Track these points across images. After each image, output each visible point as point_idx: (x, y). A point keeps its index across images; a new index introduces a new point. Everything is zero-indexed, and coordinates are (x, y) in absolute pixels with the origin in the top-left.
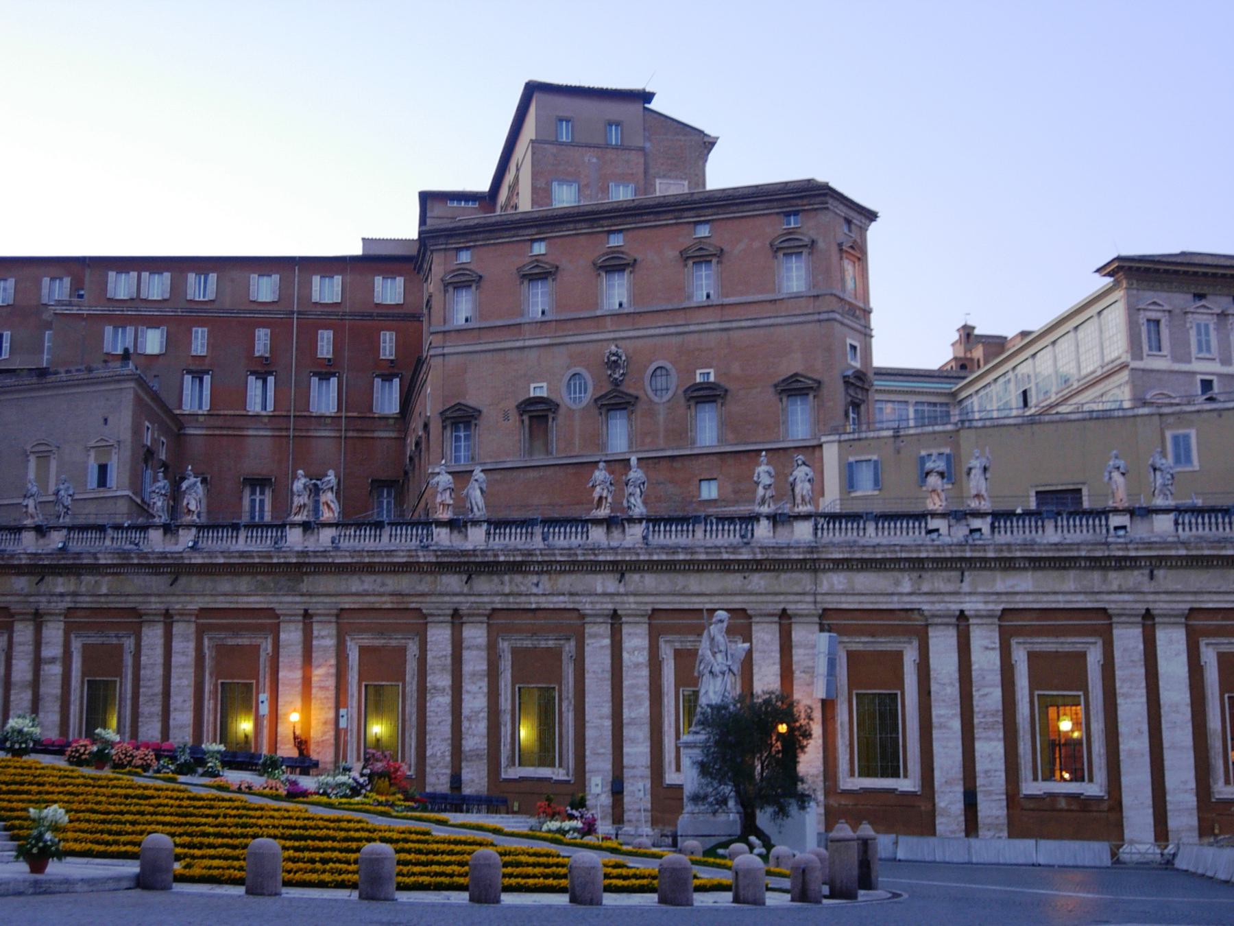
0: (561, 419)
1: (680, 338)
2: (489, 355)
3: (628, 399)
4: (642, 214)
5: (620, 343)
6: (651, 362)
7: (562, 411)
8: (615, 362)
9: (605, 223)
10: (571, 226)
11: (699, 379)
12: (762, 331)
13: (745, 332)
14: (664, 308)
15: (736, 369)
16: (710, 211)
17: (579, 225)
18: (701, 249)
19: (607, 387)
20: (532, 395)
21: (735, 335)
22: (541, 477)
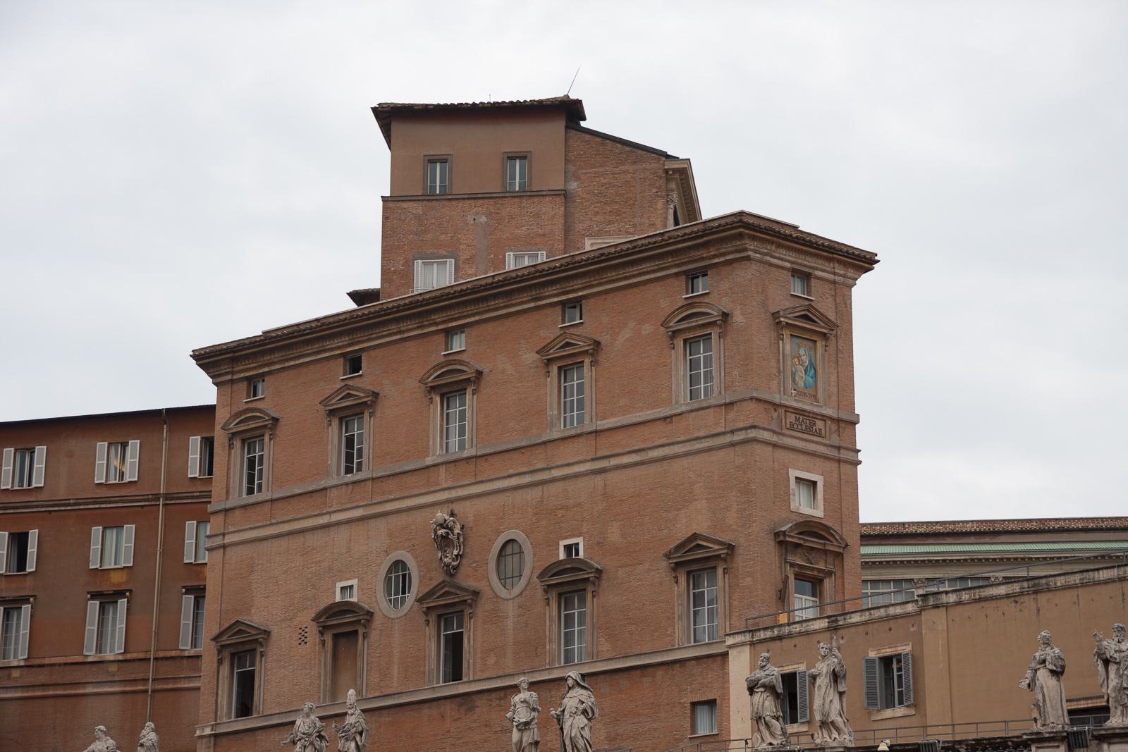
0: (374, 635)
1: (536, 493)
2: (283, 542)
3: (462, 596)
4: (486, 299)
5: (457, 508)
7: (377, 621)
9: (437, 317)
10: (393, 328)
12: (653, 469)
13: (629, 472)
14: (517, 445)
16: (578, 283)
17: (403, 326)
20: (338, 599)
21: (613, 477)
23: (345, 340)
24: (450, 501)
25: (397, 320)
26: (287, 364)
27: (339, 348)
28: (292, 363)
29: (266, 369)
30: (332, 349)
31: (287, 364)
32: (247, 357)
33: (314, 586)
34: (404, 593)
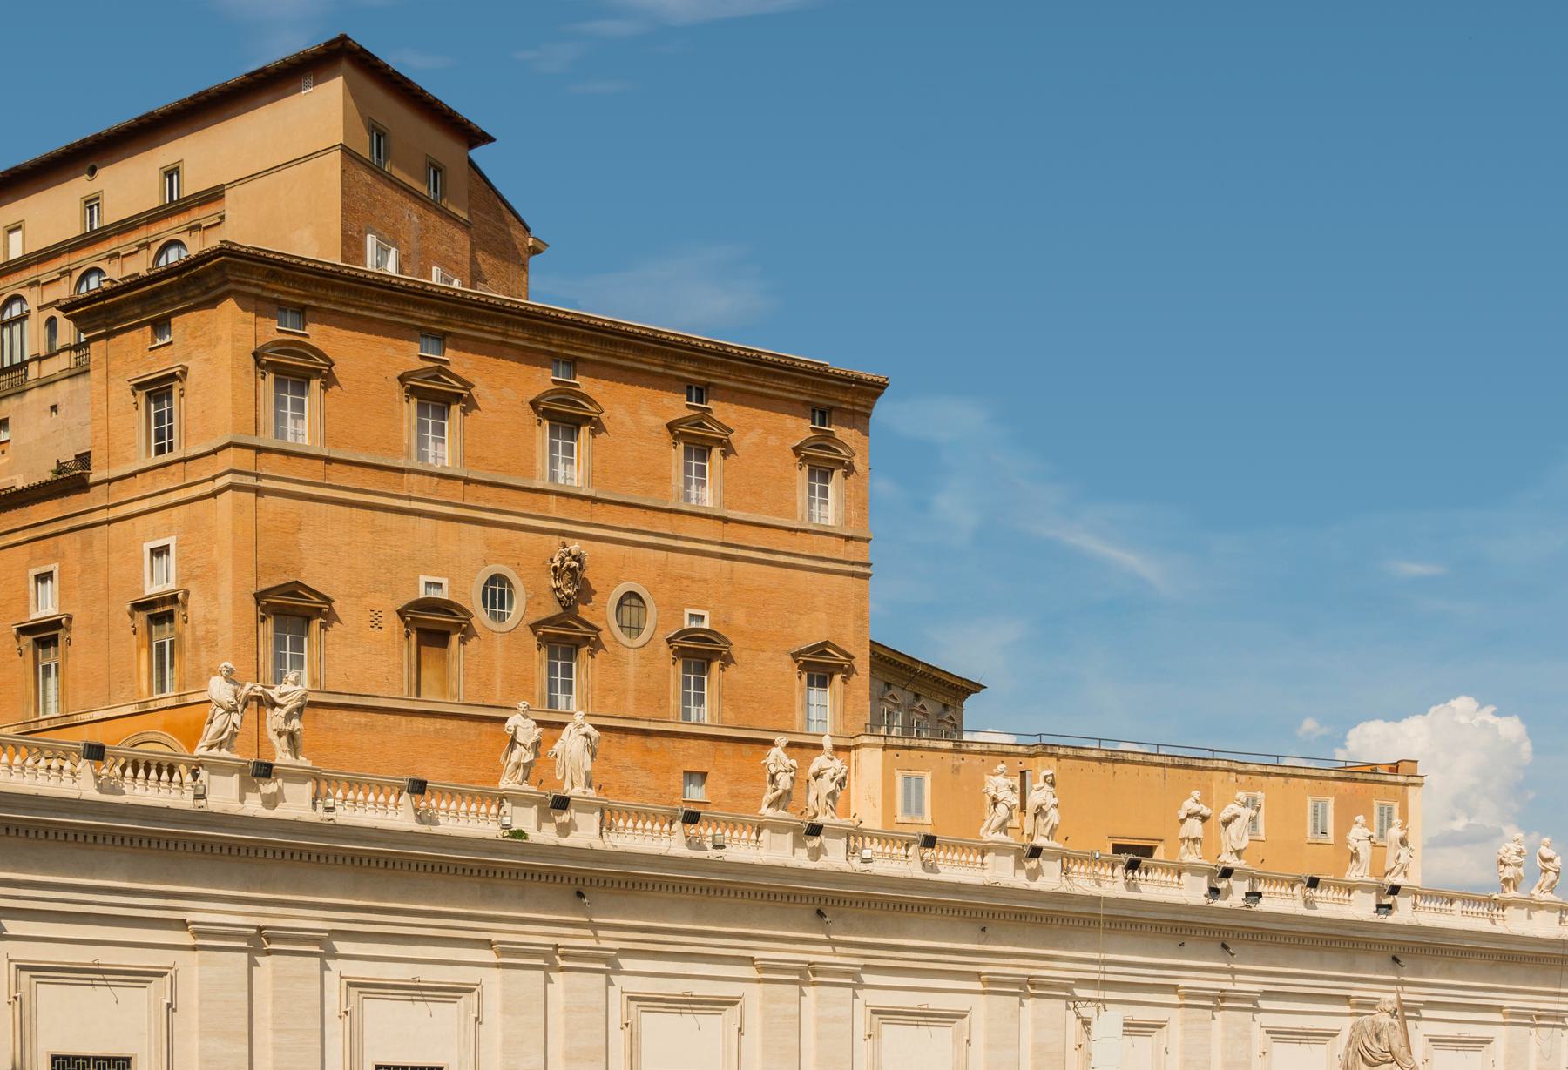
5: (568, 540)
6: (618, 581)
11: (687, 625)
15: (739, 617)
18: (700, 425)
19: (554, 609)
20: (422, 595)
22: (437, 732)
23: (434, 315)
24: (563, 533)
25: (507, 322)
26: (344, 309)
27: (421, 319)
28: (353, 311)
29: (313, 303)
30: (412, 318)
31: (344, 309)
32: (294, 280)
34: (501, 606)
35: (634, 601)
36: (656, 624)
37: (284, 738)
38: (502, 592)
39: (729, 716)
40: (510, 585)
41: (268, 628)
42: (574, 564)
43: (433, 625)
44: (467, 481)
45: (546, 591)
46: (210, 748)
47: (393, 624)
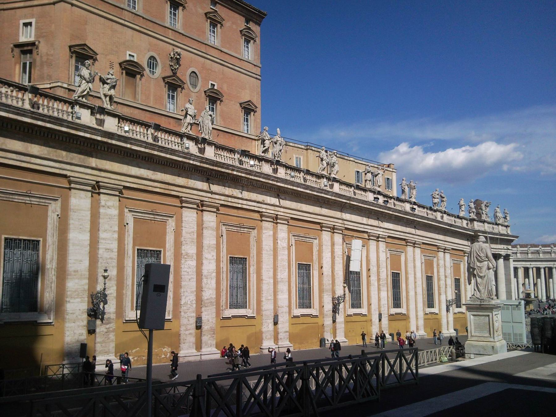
6: (190, 67)
8: (177, 59)
33: (117, 47)
34: (153, 69)
35: (194, 74)
36: (201, 86)
37: (108, 98)
38: (153, 63)
39: (222, 123)
40: (156, 61)
41: (73, 61)
42: (178, 57)
43: (131, 70)
44: (143, 18)
45: (168, 66)
46: (79, 97)
47: (117, 67)
